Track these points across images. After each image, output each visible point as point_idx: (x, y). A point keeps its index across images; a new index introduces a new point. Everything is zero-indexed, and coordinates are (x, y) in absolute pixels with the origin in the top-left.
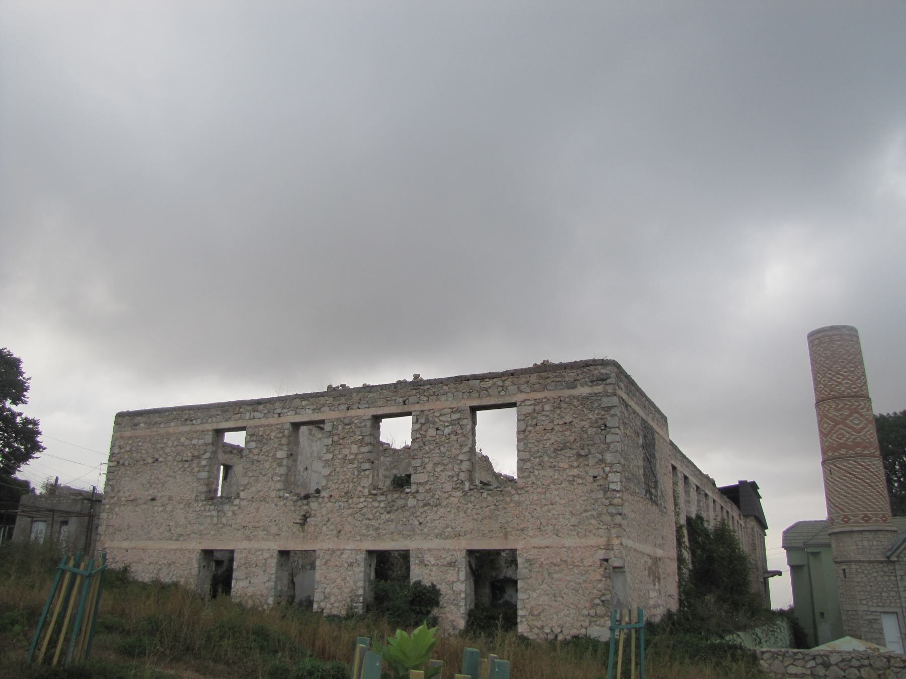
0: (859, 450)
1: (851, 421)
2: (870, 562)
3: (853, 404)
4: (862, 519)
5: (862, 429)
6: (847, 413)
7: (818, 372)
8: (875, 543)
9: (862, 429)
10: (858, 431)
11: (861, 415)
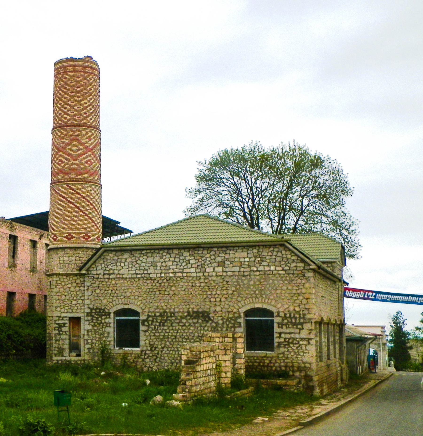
0: (73, 175)
1: (70, 149)
2: (67, 275)
3: (74, 133)
4: (66, 237)
5: (79, 156)
6: (67, 140)
7: (60, 99)
8: (74, 258)
9: (79, 156)
10: (74, 158)
11: (80, 142)
